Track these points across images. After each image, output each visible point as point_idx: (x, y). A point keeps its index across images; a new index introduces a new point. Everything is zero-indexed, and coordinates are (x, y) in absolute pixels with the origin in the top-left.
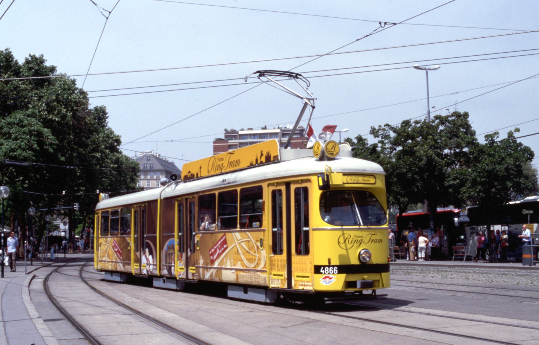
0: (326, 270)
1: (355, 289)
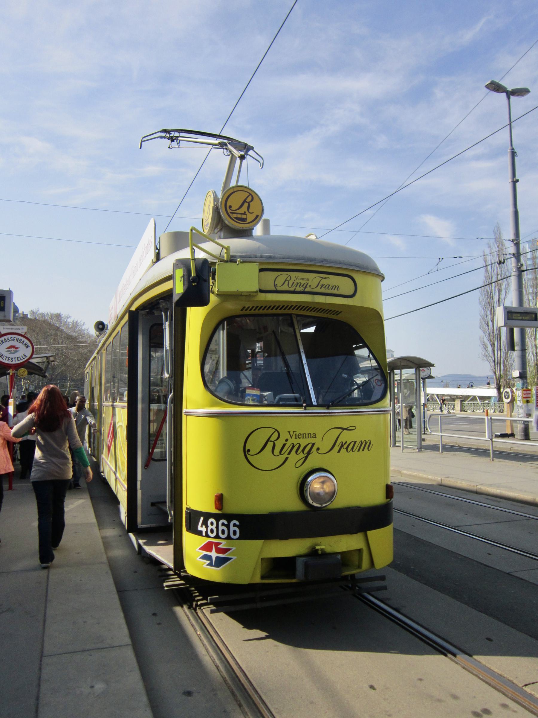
0: (210, 527)
1: (294, 581)
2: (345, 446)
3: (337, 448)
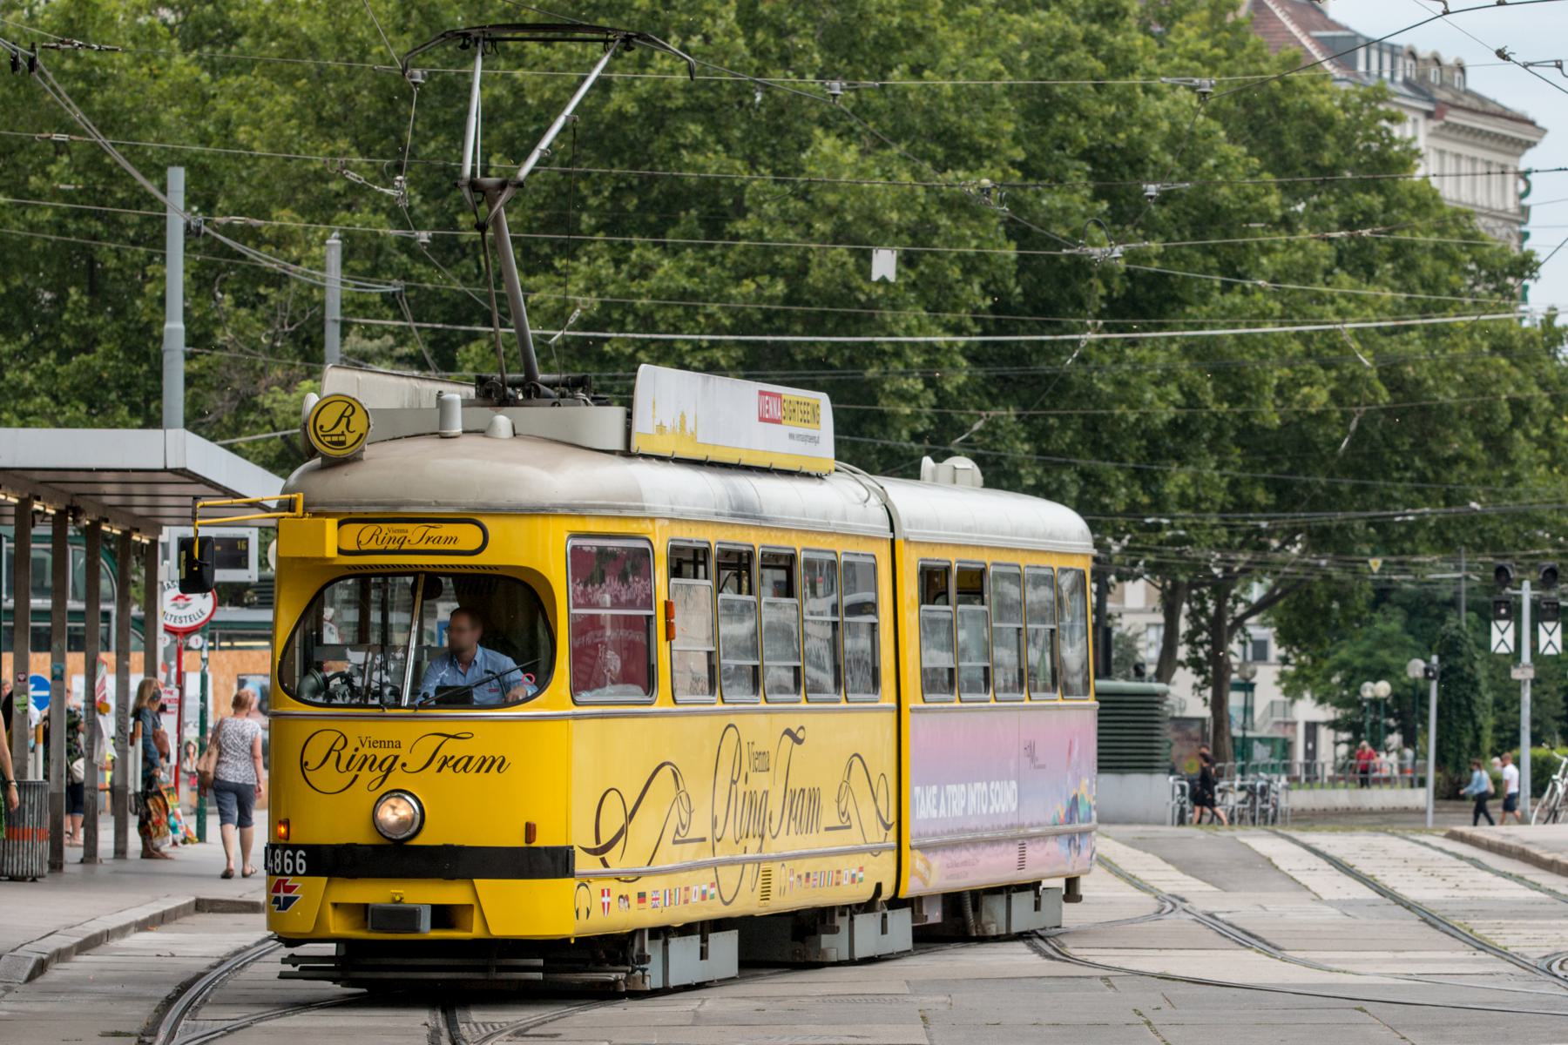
2: (451, 763)
3: (435, 765)
